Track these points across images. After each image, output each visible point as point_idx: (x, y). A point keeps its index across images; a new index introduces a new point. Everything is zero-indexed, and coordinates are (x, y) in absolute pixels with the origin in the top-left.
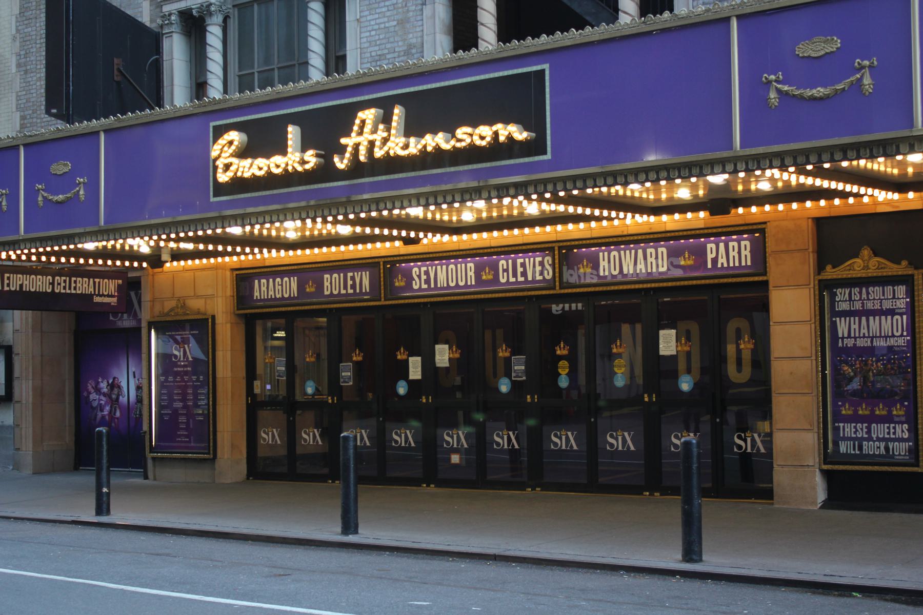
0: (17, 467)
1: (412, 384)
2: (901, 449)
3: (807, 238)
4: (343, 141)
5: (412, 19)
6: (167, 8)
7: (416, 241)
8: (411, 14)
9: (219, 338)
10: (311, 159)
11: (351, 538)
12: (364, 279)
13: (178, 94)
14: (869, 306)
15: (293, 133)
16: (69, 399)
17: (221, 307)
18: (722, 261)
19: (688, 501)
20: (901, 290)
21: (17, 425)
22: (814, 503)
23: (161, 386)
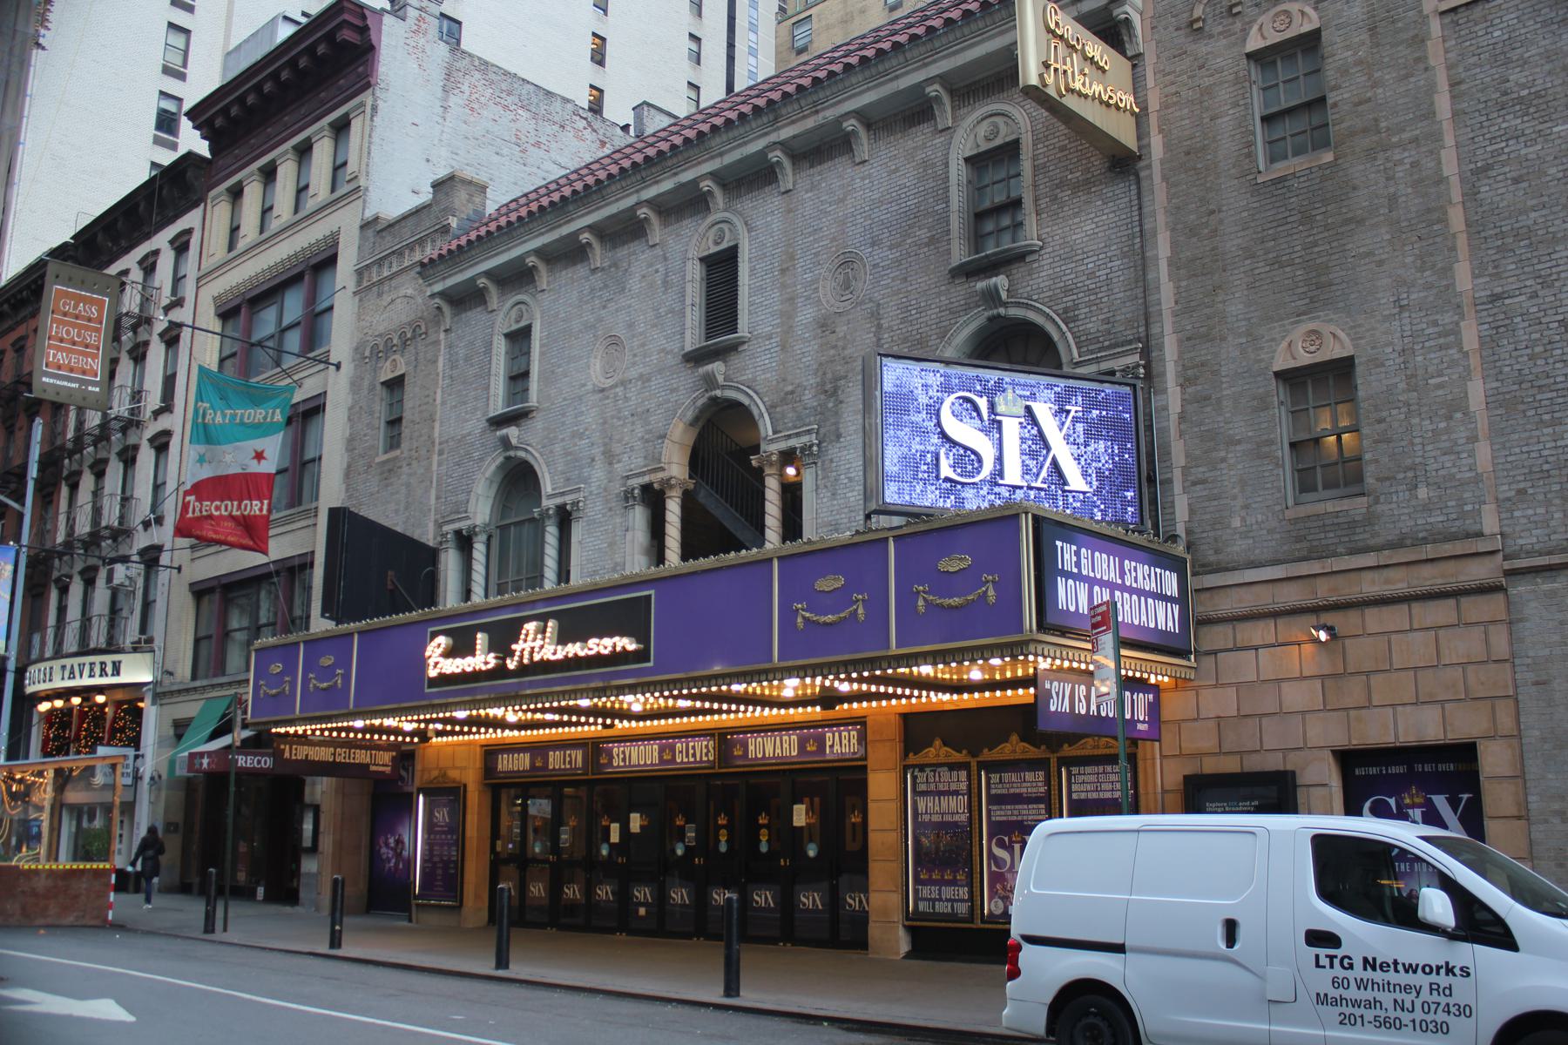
0: (317, 909)
1: (612, 846)
2: (962, 909)
3: (894, 730)
4: (514, 647)
6: (446, 528)
7: (612, 726)
9: (469, 803)
10: (492, 661)
11: (501, 973)
12: (578, 756)
13: (450, 598)
14: (941, 787)
15: (481, 639)
16: (364, 852)
17: (471, 776)
18: (837, 748)
19: (729, 947)
20: (963, 774)
21: (319, 873)
22: (898, 953)
23: (426, 842)
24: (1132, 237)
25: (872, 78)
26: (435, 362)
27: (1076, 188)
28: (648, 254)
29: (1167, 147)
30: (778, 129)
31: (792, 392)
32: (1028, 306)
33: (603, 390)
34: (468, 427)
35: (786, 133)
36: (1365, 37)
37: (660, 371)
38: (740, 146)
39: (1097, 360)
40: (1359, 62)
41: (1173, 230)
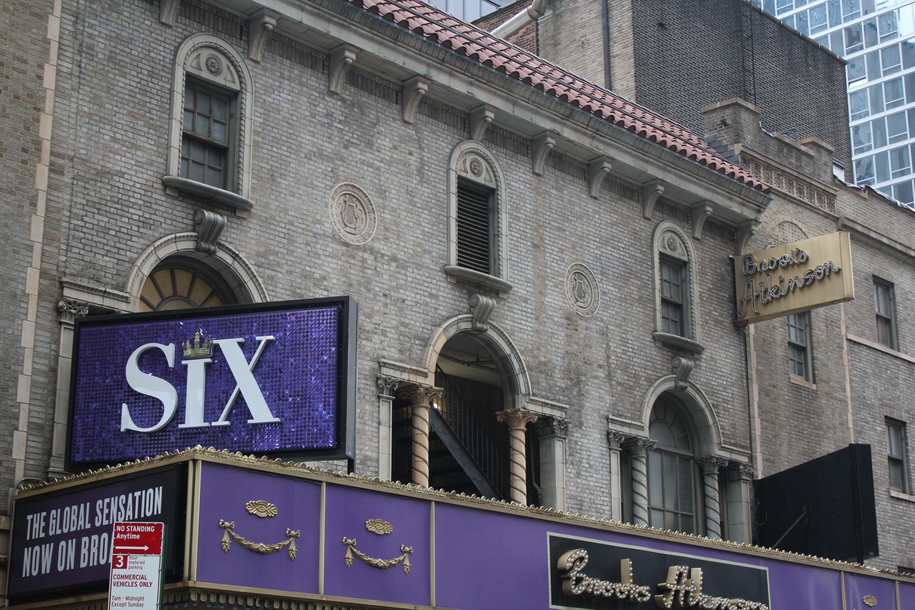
5: (368, 433)
8: (367, 428)
24: (742, 375)
25: (637, 149)
26: (43, 17)
27: (717, 322)
28: (397, 125)
29: (756, 328)
30: (564, 125)
31: (545, 364)
32: (697, 390)
33: (346, 244)
34: (117, 163)
35: (568, 134)
36: (824, 328)
37: (419, 266)
38: (532, 111)
39: (731, 451)
40: (823, 342)
41: (759, 386)
